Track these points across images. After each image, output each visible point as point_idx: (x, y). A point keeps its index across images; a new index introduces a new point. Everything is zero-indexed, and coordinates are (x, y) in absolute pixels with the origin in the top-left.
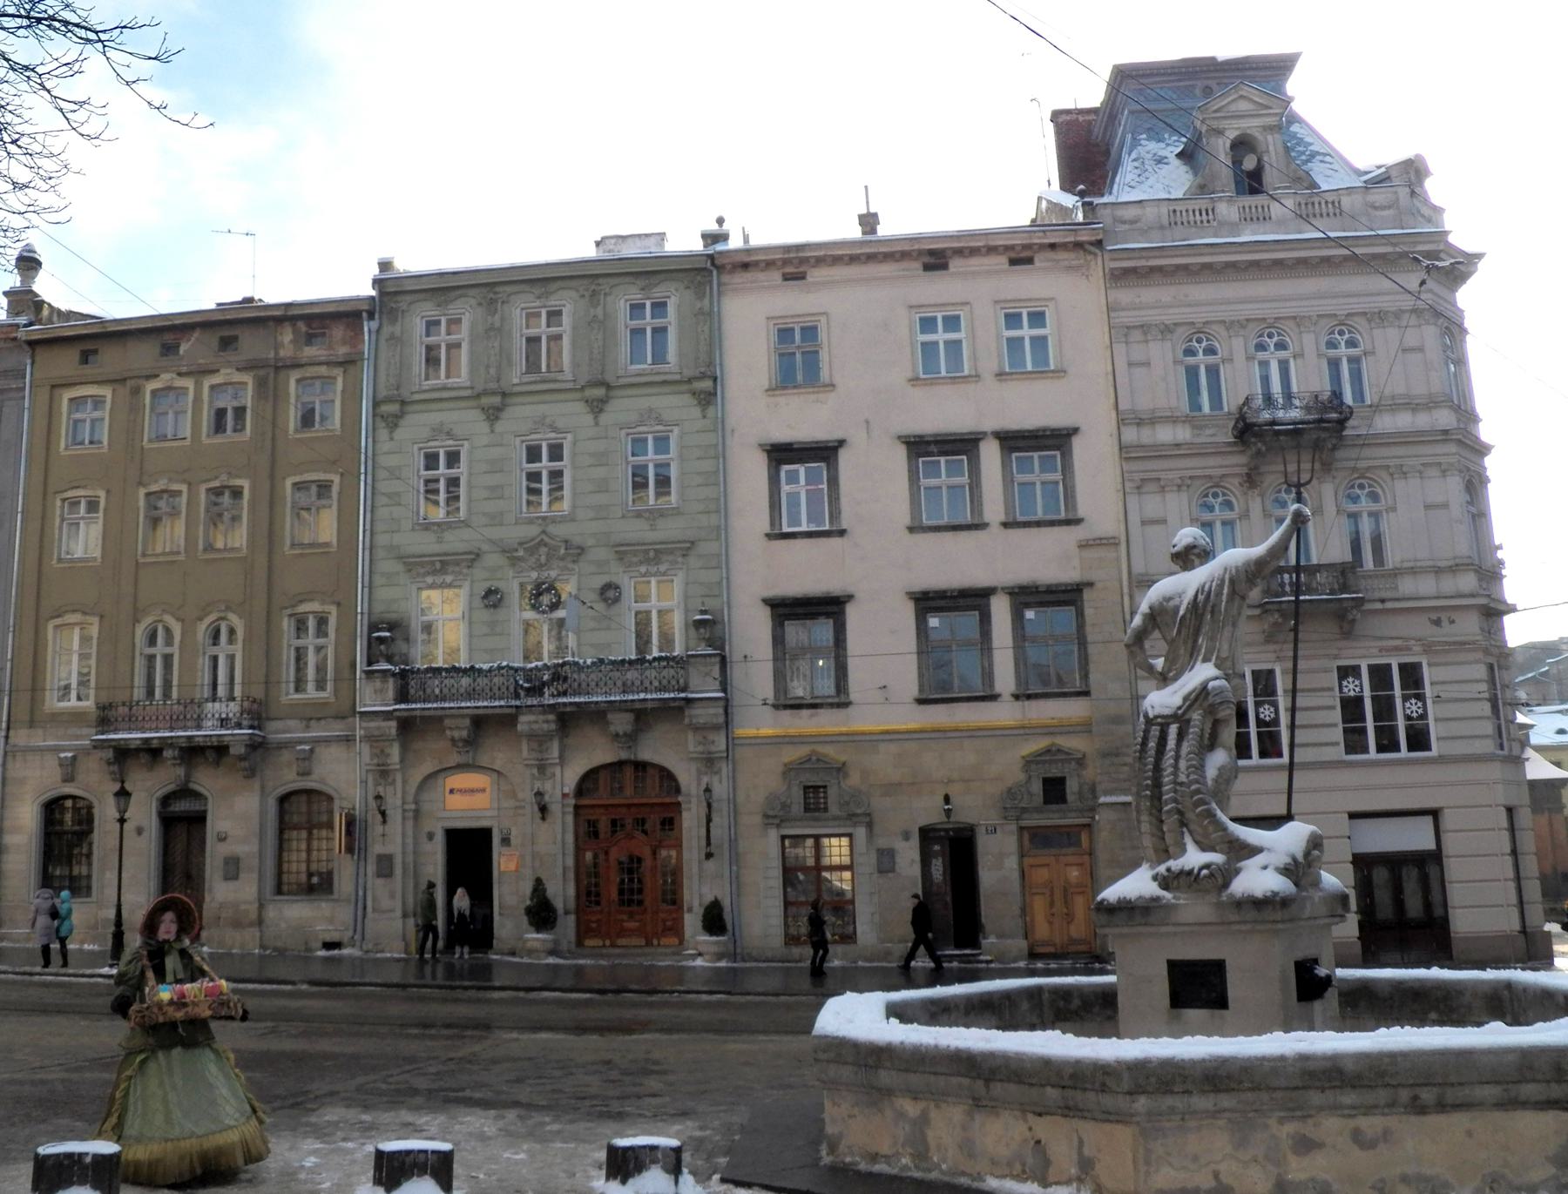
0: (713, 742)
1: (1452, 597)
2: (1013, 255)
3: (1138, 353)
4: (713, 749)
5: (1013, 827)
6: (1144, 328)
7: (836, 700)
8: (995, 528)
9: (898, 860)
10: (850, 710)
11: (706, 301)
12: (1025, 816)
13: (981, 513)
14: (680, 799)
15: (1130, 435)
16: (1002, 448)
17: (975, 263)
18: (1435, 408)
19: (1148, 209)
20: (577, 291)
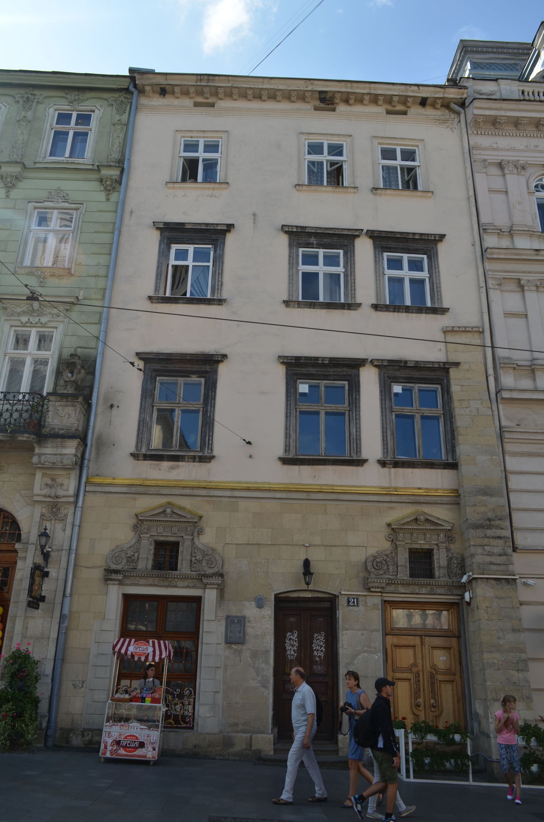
0: (62, 485)
2: (390, 108)
4: (60, 492)
5: (376, 600)
6: (501, 165)
7: (201, 454)
8: (366, 310)
9: (249, 630)
10: (213, 461)
11: (125, 117)
12: (391, 588)
13: (354, 296)
14: (17, 546)
15: (491, 241)
16: (375, 247)
17: (358, 109)
19: (502, 87)
20: (14, 97)
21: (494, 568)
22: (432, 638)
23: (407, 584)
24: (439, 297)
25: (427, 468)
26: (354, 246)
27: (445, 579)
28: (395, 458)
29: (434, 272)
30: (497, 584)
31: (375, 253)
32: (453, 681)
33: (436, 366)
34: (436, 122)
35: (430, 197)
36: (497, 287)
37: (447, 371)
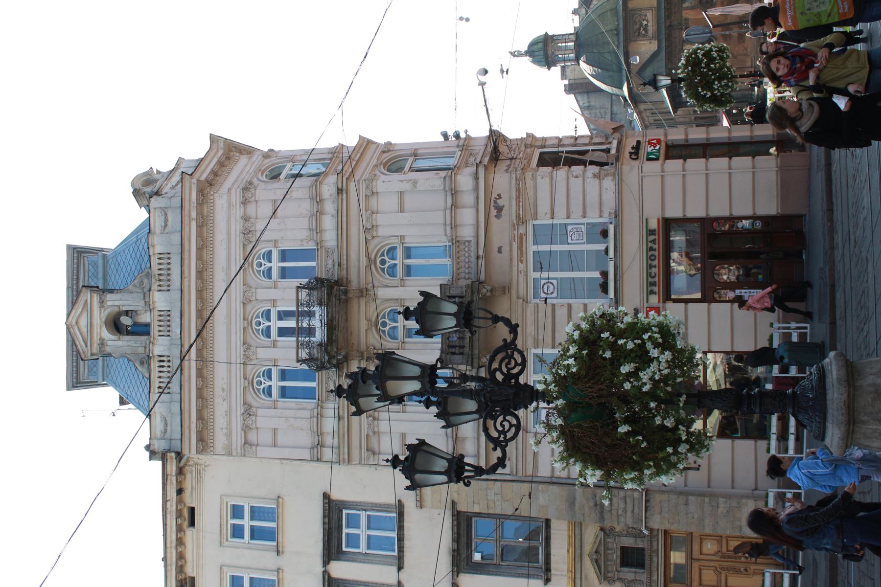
1: (477, 198)
2: (186, 524)
3: (265, 437)
6: (246, 429)
16: (338, 559)
17: (189, 555)
18: (320, 195)
21: (636, 510)
22: (693, 553)
23: (650, 575)
24: (386, 506)
25: (550, 542)
26: (338, 579)
27: (646, 542)
28: (542, 568)
29: (361, 507)
30: (650, 510)
31: (345, 560)
32: (727, 540)
33: (455, 523)
34: (200, 481)
35: (283, 499)
36: (376, 457)
37: (459, 512)
